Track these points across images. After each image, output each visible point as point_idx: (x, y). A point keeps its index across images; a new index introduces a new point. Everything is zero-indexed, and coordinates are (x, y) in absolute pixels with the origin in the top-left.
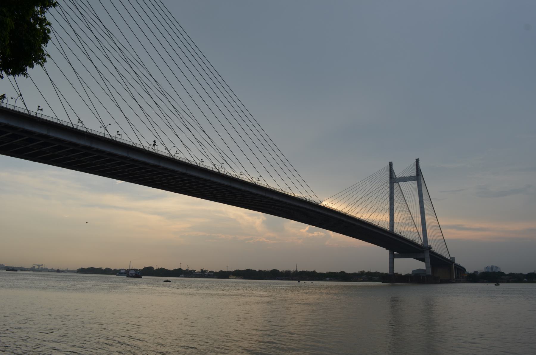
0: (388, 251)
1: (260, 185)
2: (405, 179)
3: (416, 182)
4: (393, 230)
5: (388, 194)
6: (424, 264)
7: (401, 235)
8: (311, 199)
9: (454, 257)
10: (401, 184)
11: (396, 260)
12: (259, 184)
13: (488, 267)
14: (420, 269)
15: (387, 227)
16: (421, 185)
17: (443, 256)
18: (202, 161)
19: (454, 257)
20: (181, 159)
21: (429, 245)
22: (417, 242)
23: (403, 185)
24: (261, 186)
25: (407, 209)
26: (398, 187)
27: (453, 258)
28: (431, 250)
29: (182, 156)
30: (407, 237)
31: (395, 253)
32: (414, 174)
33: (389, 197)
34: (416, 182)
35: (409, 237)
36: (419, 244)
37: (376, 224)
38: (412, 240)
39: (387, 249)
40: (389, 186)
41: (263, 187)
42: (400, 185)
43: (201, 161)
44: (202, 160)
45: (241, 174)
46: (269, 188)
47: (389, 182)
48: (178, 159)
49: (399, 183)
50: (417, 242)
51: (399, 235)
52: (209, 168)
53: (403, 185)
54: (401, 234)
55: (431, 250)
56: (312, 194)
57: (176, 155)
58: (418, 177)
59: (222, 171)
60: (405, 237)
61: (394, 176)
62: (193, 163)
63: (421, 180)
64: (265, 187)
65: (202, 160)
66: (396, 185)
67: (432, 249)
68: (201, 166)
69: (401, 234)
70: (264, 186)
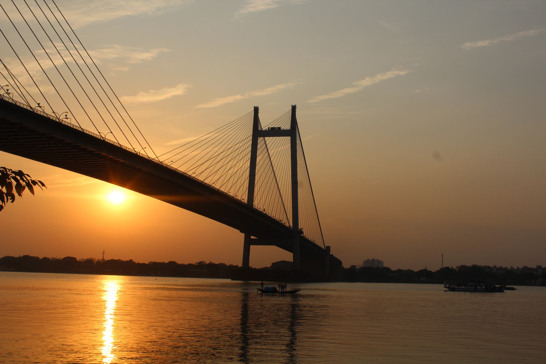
0: (243, 235)
2: (275, 132)
6: (291, 255)
7: (265, 212)
9: (330, 247)
11: (252, 247)
12: (66, 124)
13: (368, 260)
14: (283, 261)
15: (245, 199)
17: (316, 244)
19: (330, 247)
21: (300, 228)
22: (285, 223)
27: (328, 248)
28: (302, 235)
30: (272, 216)
31: (252, 237)
35: (274, 216)
36: (287, 226)
38: (278, 220)
41: (126, 150)
50: (285, 223)
51: (261, 212)
54: (264, 211)
55: (302, 235)
60: (270, 215)
61: (260, 129)
63: (296, 136)
64: (128, 151)
67: (303, 234)
69: (259, 209)
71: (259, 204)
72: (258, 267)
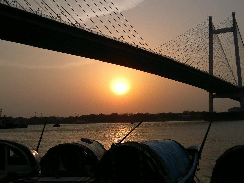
1: (95, 33)
3: (232, 32)
4: (213, 74)
5: (209, 43)
8: (142, 46)
10: (219, 35)
12: (93, 32)
15: (207, 71)
16: (237, 35)
18: (38, 10)
20: (18, 7)
23: (221, 36)
24: (96, 34)
25: (225, 57)
26: (217, 38)
29: (18, 5)
32: (231, 26)
33: (209, 45)
34: (232, 32)
37: (199, 68)
39: (207, 91)
40: (209, 35)
42: (218, 36)
43: (37, 9)
44: (38, 8)
45: (76, 23)
46: (103, 36)
47: (209, 33)
48: (15, 7)
49: (218, 34)
52: (45, 16)
53: (221, 36)
56: (142, 43)
57: (13, 3)
58: (234, 29)
59: (58, 20)
62: (29, 11)
65: (38, 8)
66: (215, 36)
68: (38, 14)
70: (98, 34)
71: (216, 73)
72: (217, 112)
